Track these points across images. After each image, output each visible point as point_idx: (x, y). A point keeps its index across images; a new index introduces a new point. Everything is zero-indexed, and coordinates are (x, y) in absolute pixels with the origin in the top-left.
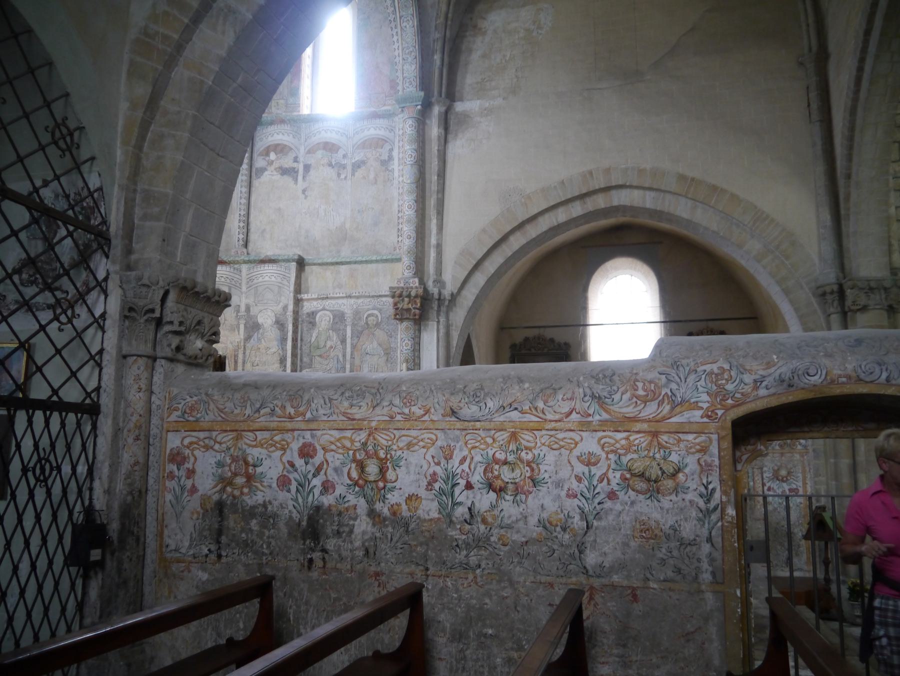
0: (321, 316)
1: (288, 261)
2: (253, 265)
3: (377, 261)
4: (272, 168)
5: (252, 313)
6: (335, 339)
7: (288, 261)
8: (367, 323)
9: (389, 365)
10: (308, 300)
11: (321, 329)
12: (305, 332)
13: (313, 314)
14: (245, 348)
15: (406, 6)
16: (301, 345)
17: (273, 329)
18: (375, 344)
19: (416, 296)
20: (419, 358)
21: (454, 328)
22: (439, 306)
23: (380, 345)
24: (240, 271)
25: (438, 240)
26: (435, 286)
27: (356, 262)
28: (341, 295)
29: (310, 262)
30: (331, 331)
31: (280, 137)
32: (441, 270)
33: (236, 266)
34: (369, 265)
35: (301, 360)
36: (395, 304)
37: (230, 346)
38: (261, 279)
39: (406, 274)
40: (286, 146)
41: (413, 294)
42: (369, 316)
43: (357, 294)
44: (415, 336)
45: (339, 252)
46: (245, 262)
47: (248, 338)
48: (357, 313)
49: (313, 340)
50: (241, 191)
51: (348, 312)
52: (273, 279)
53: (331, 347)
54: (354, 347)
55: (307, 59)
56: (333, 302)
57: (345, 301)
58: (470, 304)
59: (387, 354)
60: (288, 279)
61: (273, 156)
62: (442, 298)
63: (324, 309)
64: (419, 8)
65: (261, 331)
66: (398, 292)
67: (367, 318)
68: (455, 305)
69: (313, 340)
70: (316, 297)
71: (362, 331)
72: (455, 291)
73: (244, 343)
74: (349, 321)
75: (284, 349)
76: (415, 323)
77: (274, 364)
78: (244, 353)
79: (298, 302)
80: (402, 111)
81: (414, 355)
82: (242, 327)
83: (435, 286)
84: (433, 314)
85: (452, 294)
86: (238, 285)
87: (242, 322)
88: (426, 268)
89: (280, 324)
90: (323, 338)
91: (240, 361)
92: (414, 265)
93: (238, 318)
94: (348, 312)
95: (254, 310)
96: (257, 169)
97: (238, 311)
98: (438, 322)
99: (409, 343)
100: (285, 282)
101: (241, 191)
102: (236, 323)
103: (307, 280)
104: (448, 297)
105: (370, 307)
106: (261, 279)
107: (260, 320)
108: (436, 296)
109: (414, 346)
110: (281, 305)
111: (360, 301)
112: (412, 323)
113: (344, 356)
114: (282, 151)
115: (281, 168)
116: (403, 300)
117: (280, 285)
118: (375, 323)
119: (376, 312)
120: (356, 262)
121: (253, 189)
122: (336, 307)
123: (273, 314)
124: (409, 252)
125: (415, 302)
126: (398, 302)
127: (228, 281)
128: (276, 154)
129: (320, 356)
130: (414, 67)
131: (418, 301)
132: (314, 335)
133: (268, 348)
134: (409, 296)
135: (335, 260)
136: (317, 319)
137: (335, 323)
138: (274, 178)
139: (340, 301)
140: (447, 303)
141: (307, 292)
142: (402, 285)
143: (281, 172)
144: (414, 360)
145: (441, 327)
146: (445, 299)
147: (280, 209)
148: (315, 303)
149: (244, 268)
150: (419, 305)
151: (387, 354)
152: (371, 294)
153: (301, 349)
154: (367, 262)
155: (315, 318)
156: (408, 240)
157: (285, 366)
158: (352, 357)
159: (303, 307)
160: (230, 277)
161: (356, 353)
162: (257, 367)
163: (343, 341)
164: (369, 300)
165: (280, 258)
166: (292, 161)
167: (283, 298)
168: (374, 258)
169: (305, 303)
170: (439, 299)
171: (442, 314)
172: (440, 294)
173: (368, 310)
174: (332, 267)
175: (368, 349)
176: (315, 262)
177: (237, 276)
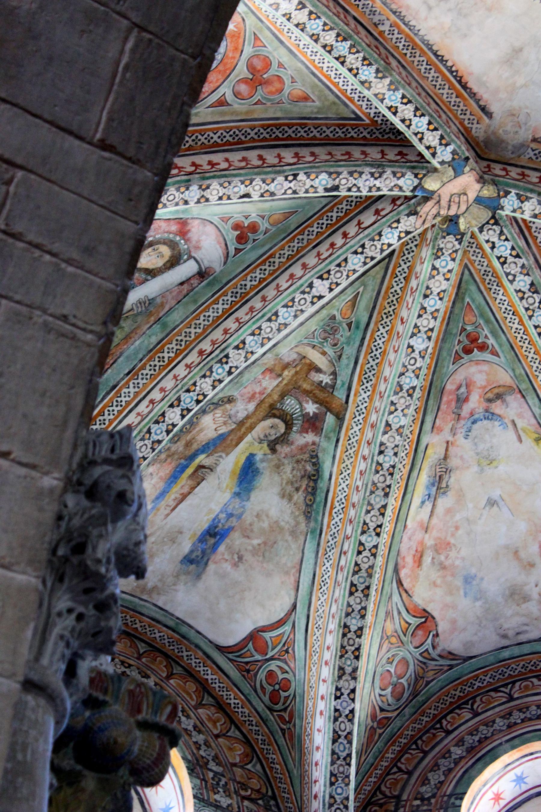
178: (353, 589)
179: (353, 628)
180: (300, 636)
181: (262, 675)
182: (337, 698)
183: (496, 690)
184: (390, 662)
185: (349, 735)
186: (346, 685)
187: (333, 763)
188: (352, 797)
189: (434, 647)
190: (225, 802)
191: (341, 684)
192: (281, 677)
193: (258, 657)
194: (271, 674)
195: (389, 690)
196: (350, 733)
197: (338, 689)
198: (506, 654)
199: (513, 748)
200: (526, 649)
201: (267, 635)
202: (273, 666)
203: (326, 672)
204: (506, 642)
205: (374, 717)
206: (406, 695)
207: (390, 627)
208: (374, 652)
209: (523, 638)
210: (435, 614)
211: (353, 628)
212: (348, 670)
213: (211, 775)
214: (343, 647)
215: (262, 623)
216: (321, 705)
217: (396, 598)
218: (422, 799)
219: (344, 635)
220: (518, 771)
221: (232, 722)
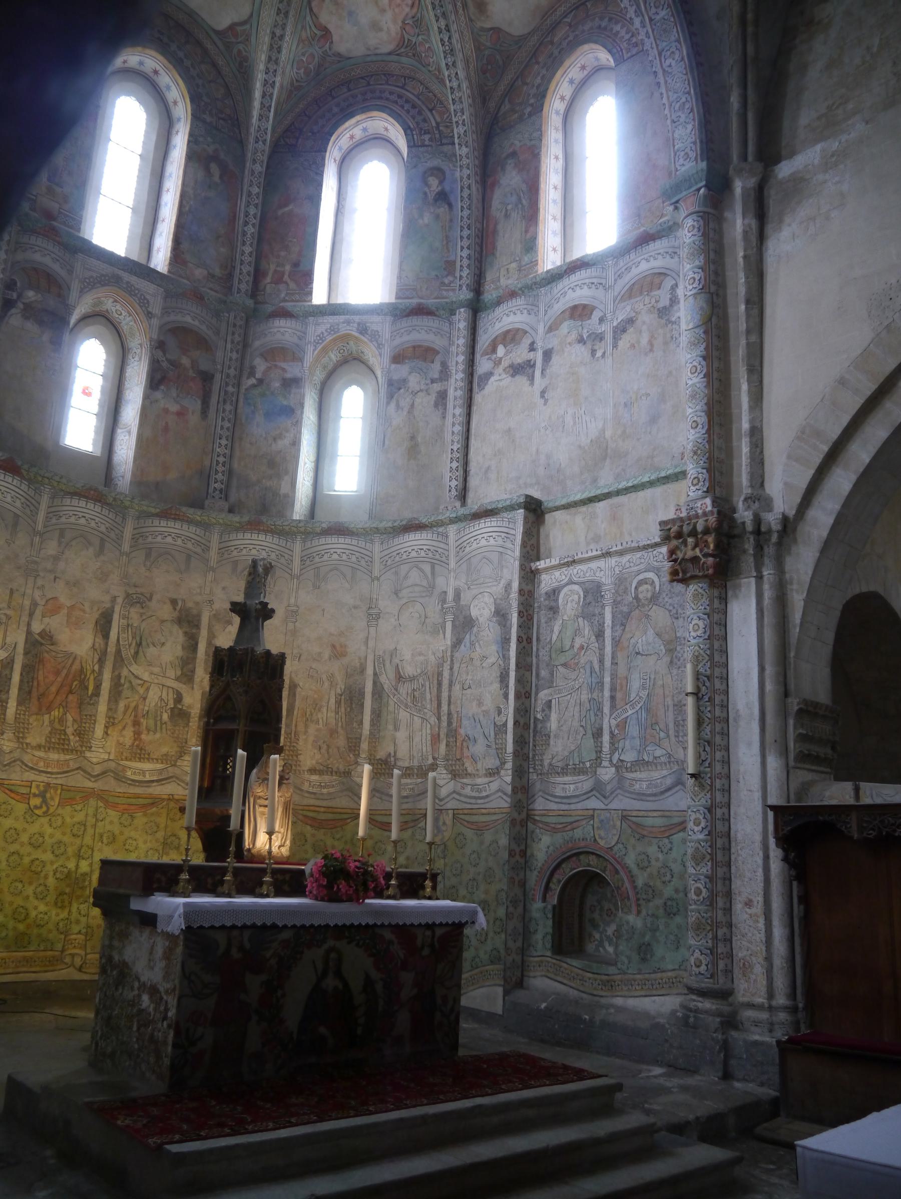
0: (566, 595)
1: (511, 508)
2: (462, 525)
3: (651, 484)
4: (501, 367)
5: (462, 603)
6: (586, 632)
7: (511, 508)
8: (636, 598)
9: (675, 672)
10: (547, 569)
11: (565, 618)
12: (543, 625)
13: (554, 593)
14: (452, 660)
15: (665, 30)
16: (538, 649)
17: (491, 624)
18: (651, 633)
19: (707, 531)
20: (725, 652)
21: (795, 587)
22: (759, 548)
23: (658, 635)
24: (447, 537)
25: (751, 421)
26: (748, 508)
27: (618, 493)
28: (595, 553)
29: (551, 505)
30: (580, 620)
31: (512, 318)
32: (762, 476)
33: (440, 530)
34: (641, 494)
35: (538, 675)
36: (672, 552)
37: (432, 658)
38: (475, 546)
39: (691, 494)
40: (518, 329)
41: (700, 528)
42: (640, 583)
43: (619, 547)
44: (713, 610)
45: (595, 480)
46: (453, 521)
47: (457, 643)
48: (621, 581)
49: (554, 637)
50: (454, 415)
51: (607, 581)
52: (492, 542)
53: (582, 647)
54: (616, 643)
55: (552, 191)
56: (583, 567)
57: (601, 563)
58: (825, 534)
59: (671, 650)
60: (512, 537)
61: (501, 351)
62: (763, 529)
63: (571, 582)
64: (690, 24)
65: (475, 629)
66: (675, 529)
67: (636, 588)
68: (795, 541)
69: (554, 637)
70: (557, 562)
71: (629, 613)
72: (791, 513)
73: (452, 652)
74: (608, 597)
75: (506, 658)
76: (712, 585)
77: (491, 683)
78: (451, 669)
79: (529, 576)
80: (676, 208)
81: (711, 648)
82: (449, 626)
83: (748, 508)
84: (748, 561)
85: (785, 519)
86: (444, 559)
87: (450, 617)
88: (735, 479)
89: (500, 615)
90: (569, 633)
91: (445, 683)
92: (706, 476)
93: (444, 612)
94: (607, 581)
95: (465, 598)
96: (480, 377)
97: (444, 601)
98: (759, 578)
99: (701, 624)
100: (510, 545)
101: (454, 415)
102: (440, 621)
103: (547, 536)
104: (776, 526)
105: (642, 567)
106: (475, 546)
107: (474, 613)
108: (749, 527)
109: (712, 629)
110: (503, 582)
111: (625, 559)
112: (705, 586)
113: (601, 661)
114: (513, 340)
115: (511, 366)
116: (685, 543)
117: (501, 550)
118: (649, 595)
119: (651, 575)
120: (618, 493)
121: (474, 408)
122: (589, 576)
123: (492, 599)
124: (695, 453)
125: (706, 541)
126: (677, 548)
127: (430, 555)
128: (505, 347)
129: (565, 665)
130: (690, 127)
131: (711, 539)
132: (556, 629)
133: (484, 658)
134: (693, 533)
135: (586, 495)
136: (560, 601)
137: (587, 604)
138: (501, 384)
139: (594, 565)
140: (774, 538)
141: (549, 556)
142: (684, 514)
143: (511, 372)
144: (711, 657)
145: (766, 586)
146: (770, 531)
147: (509, 430)
148: (557, 574)
149: (452, 529)
150: (712, 546)
151: (670, 651)
152: (641, 544)
153: (537, 656)
154: (635, 488)
155: (557, 600)
156: (692, 431)
157: (507, 686)
158: (614, 663)
159: (540, 582)
160: (432, 548)
161: (619, 654)
162: (469, 691)
163: (600, 635)
164: (639, 554)
165: (500, 506)
166: (526, 351)
167: (505, 571)
168: (646, 479)
169: (544, 577)
170: (757, 532)
171: (766, 560)
172: (758, 521)
173: (639, 573)
174: (583, 509)
175: (639, 645)
176: (558, 504)
177: (442, 545)
178: (279, 12)
179: (278, 35)
180: (254, 31)
181: (235, 51)
182: (266, 73)
183: (362, 78)
184: (303, 54)
185: (271, 95)
186: (272, 67)
187: (261, 109)
188: (270, 128)
189: (330, 49)
190: (208, 119)
191: (269, 66)
192: (244, 53)
193: (233, 40)
194: (239, 51)
195: (302, 70)
196: (272, 94)
197: (267, 68)
198: (369, 59)
199: (363, 112)
200: (379, 58)
201: (239, 29)
202: (241, 47)
203: (263, 57)
204: (369, 53)
205: (292, 84)
206: (312, 74)
207: (304, 35)
208: (294, 48)
209: (378, 51)
210: (332, 29)
211: (278, 35)
212: (274, 58)
213: (203, 103)
214: (271, 45)
215: (236, 20)
216: (260, 76)
217: (308, 18)
218: (313, 133)
219: (272, 38)
220: (364, 125)
221: (220, 73)
